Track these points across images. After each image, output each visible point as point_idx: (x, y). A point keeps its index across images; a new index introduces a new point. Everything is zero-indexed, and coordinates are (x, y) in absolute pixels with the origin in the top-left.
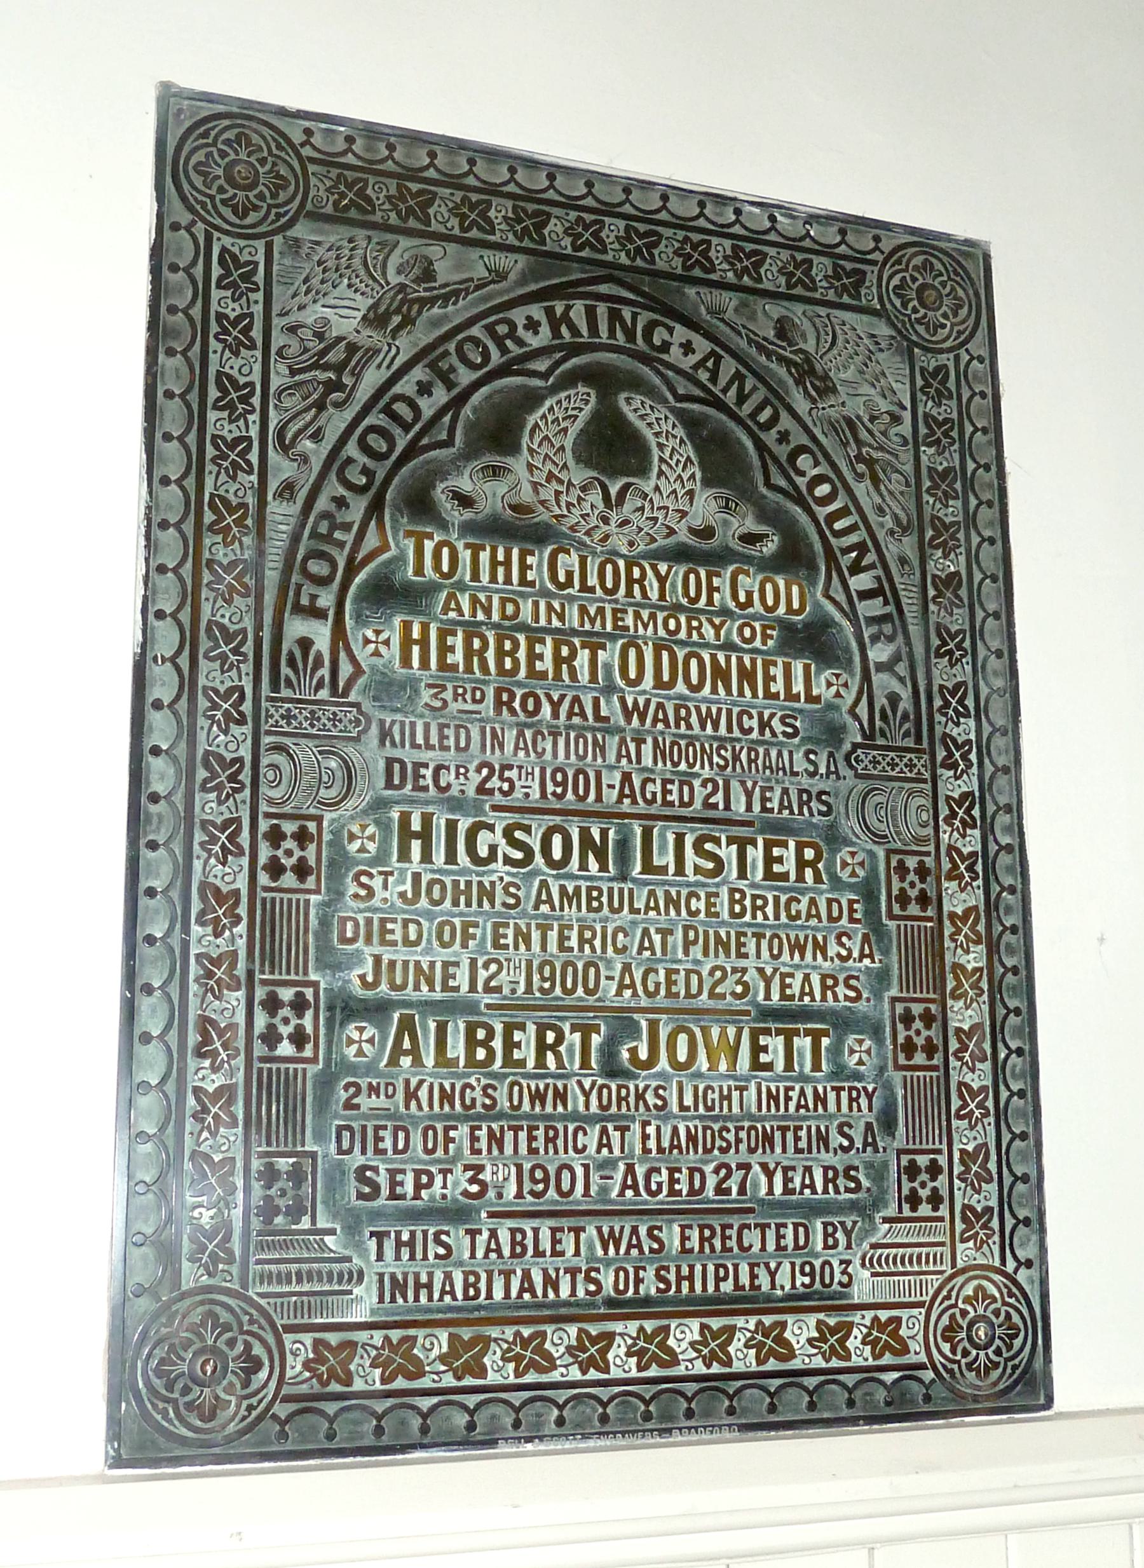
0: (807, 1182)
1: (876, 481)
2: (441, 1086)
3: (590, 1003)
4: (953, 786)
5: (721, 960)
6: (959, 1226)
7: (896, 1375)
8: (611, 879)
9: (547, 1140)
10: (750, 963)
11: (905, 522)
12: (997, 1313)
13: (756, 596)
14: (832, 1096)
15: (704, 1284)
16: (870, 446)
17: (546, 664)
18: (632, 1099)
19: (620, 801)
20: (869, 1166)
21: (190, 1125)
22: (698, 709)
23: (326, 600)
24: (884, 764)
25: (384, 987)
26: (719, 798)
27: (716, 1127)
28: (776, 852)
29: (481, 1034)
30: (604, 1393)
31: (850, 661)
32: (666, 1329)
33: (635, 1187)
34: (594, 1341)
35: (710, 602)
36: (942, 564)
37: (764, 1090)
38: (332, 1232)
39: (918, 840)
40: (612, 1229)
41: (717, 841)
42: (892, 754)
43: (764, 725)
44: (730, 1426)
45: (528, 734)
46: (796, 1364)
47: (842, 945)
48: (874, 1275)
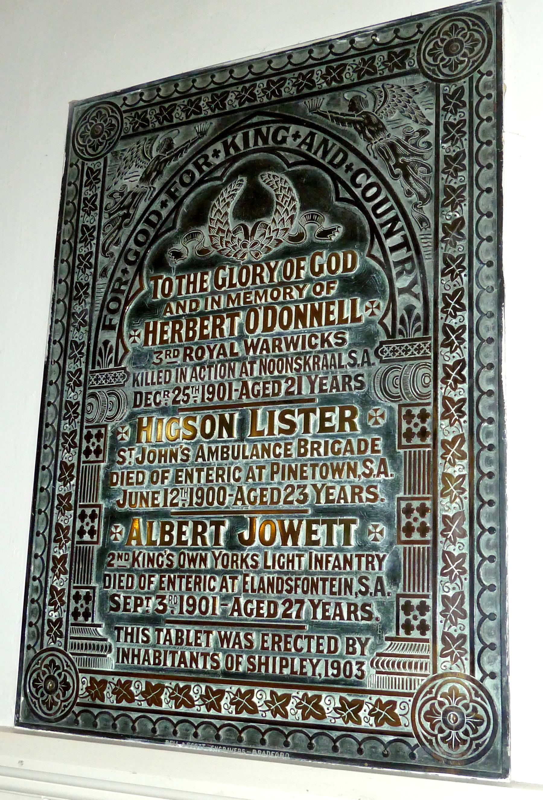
0: (338, 612)
1: (406, 176)
2: (149, 554)
3: (222, 510)
4: (448, 357)
5: (292, 481)
6: (440, 646)
7: (392, 738)
8: (236, 441)
9: (196, 583)
10: (309, 482)
11: (425, 196)
12: (466, 707)
13: (325, 266)
14: (355, 560)
15: (274, 668)
16: (405, 155)
17: (208, 331)
18: (239, 562)
19: (240, 398)
20: (380, 604)
21: (51, 574)
22: (286, 339)
23: (116, 321)
24: (400, 351)
25: (127, 506)
26: (295, 388)
27: (285, 578)
28: (328, 415)
29: (167, 528)
30: (217, 723)
31: (384, 292)
32: (252, 692)
33: (239, 610)
34: (214, 693)
35: (298, 276)
36: (448, 216)
37: (313, 556)
38: (99, 626)
39: (421, 396)
40: (226, 633)
41: (292, 413)
42: (406, 344)
43: (324, 340)
44: (285, 753)
45: (198, 368)
46: (326, 722)
47: (367, 467)
48: (377, 672)
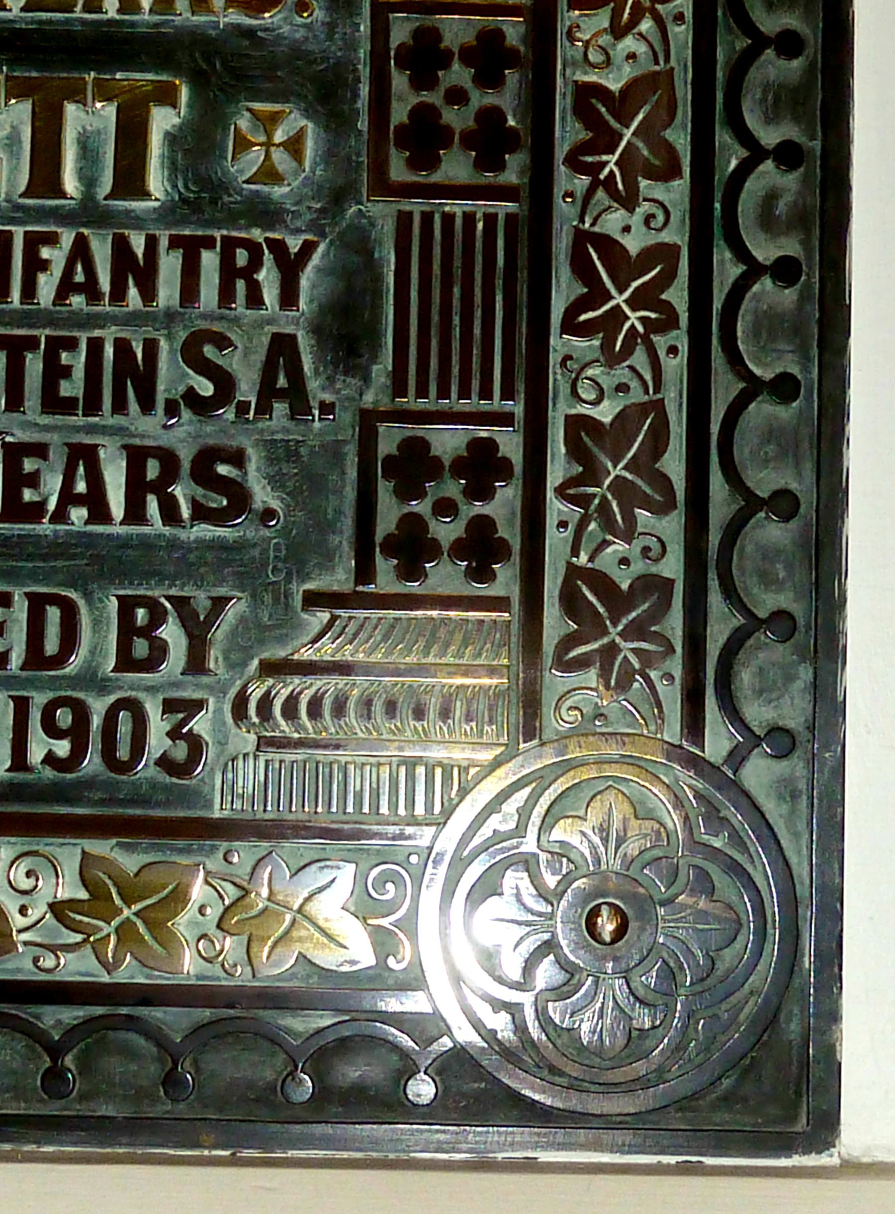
14: (170, 264)
20: (280, 453)
48: (263, 743)
